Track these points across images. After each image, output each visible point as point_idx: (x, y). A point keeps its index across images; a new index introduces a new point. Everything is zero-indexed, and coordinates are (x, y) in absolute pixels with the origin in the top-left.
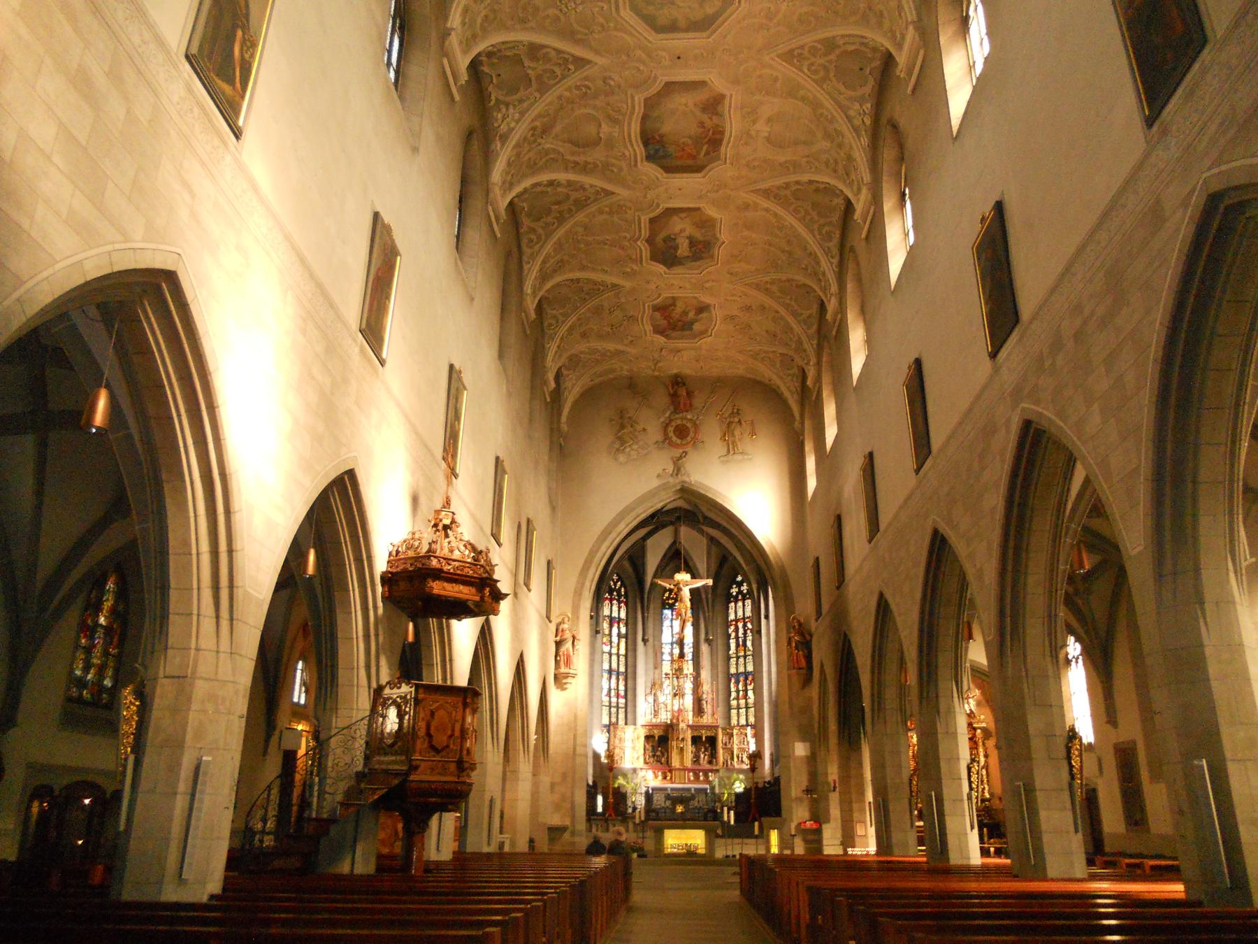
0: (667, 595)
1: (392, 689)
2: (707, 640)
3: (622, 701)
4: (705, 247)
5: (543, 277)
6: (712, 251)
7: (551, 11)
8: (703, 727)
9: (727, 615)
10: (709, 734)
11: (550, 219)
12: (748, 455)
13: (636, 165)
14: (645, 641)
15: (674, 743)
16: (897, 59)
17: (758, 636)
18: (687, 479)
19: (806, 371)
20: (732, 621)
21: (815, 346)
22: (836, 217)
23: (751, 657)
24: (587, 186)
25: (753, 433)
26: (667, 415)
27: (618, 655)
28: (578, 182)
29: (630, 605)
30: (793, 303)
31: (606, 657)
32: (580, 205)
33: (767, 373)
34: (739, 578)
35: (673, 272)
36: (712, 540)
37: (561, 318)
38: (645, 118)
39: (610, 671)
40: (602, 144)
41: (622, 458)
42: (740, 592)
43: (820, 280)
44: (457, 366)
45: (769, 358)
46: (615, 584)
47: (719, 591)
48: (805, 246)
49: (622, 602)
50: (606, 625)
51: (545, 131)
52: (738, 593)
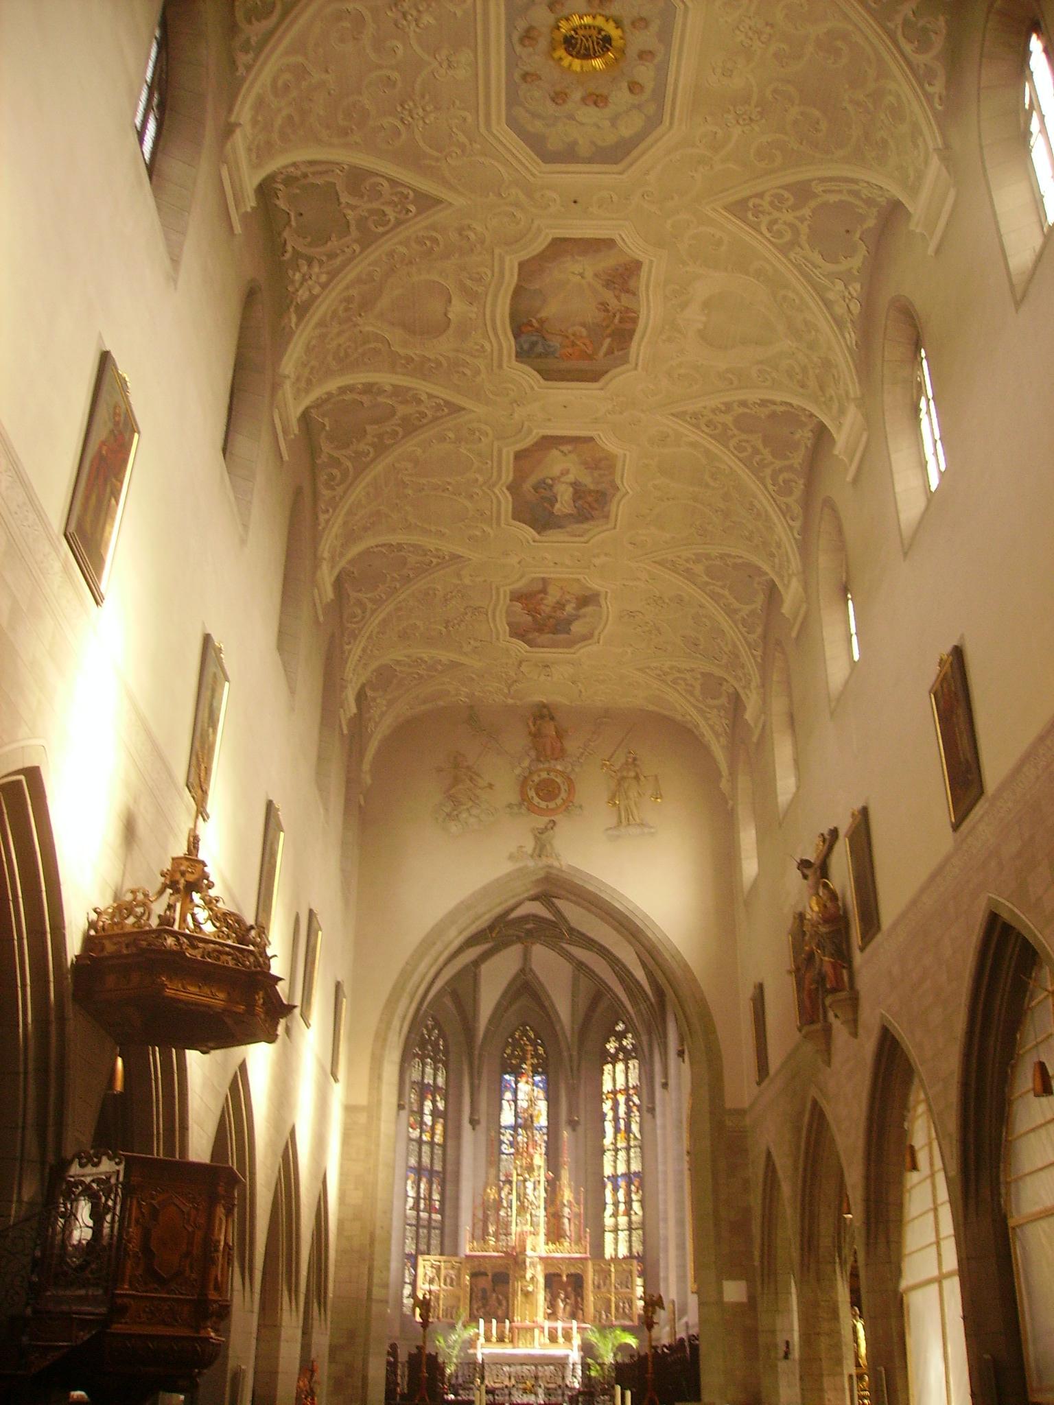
0: (508, 1051)
1: (82, 1166)
4: (596, 501)
5: (350, 537)
6: (606, 509)
7: (388, 121)
10: (573, 1271)
11: (362, 447)
12: (652, 827)
13: (500, 366)
14: (474, 1122)
15: (519, 1285)
16: (911, 210)
18: (556, 864)
19: (743, 697)
21: (759, 660)
22: (798, 459)
23: (638, 1150)
24: (424, 397)
25: (658, 795)
26: (526, 763)
27: (432, 1144)
28: (410, 389)
30: (726, 593)
31: (414, 1146)
32: (410, 427)
33: (682, 706)
34: (620, 1027)
35: (544, 539)
36: (580, 966)
37: (370, 605)
38: (518, 292)
40: (451, 331)
41: (454, 828)
42: (621, 1048)
43: (773, 555)
44: (217, 640)
45: (685, 680)
48: (751, 503)
49: (440, 1061)
51: (366, 305)
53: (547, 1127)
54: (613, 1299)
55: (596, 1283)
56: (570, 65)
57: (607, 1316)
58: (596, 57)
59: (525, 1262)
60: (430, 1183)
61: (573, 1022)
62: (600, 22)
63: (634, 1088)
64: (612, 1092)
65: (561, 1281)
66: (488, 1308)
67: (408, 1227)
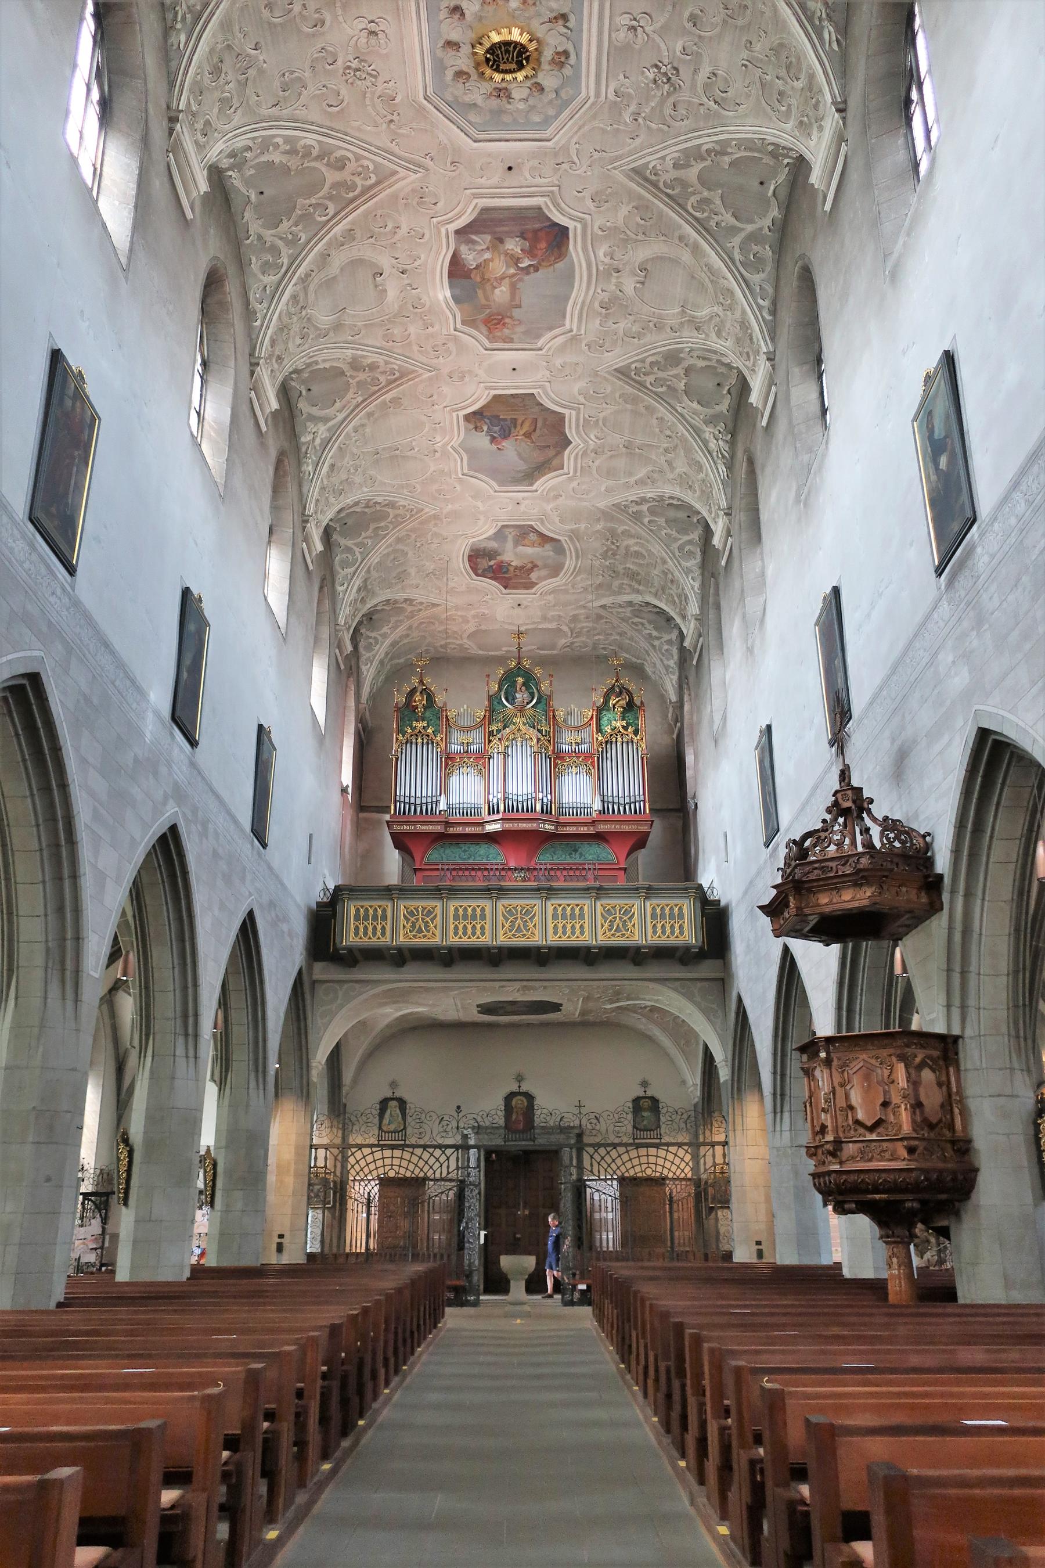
56: (521, 34)
58: (499, 43)
62: (498, 77)
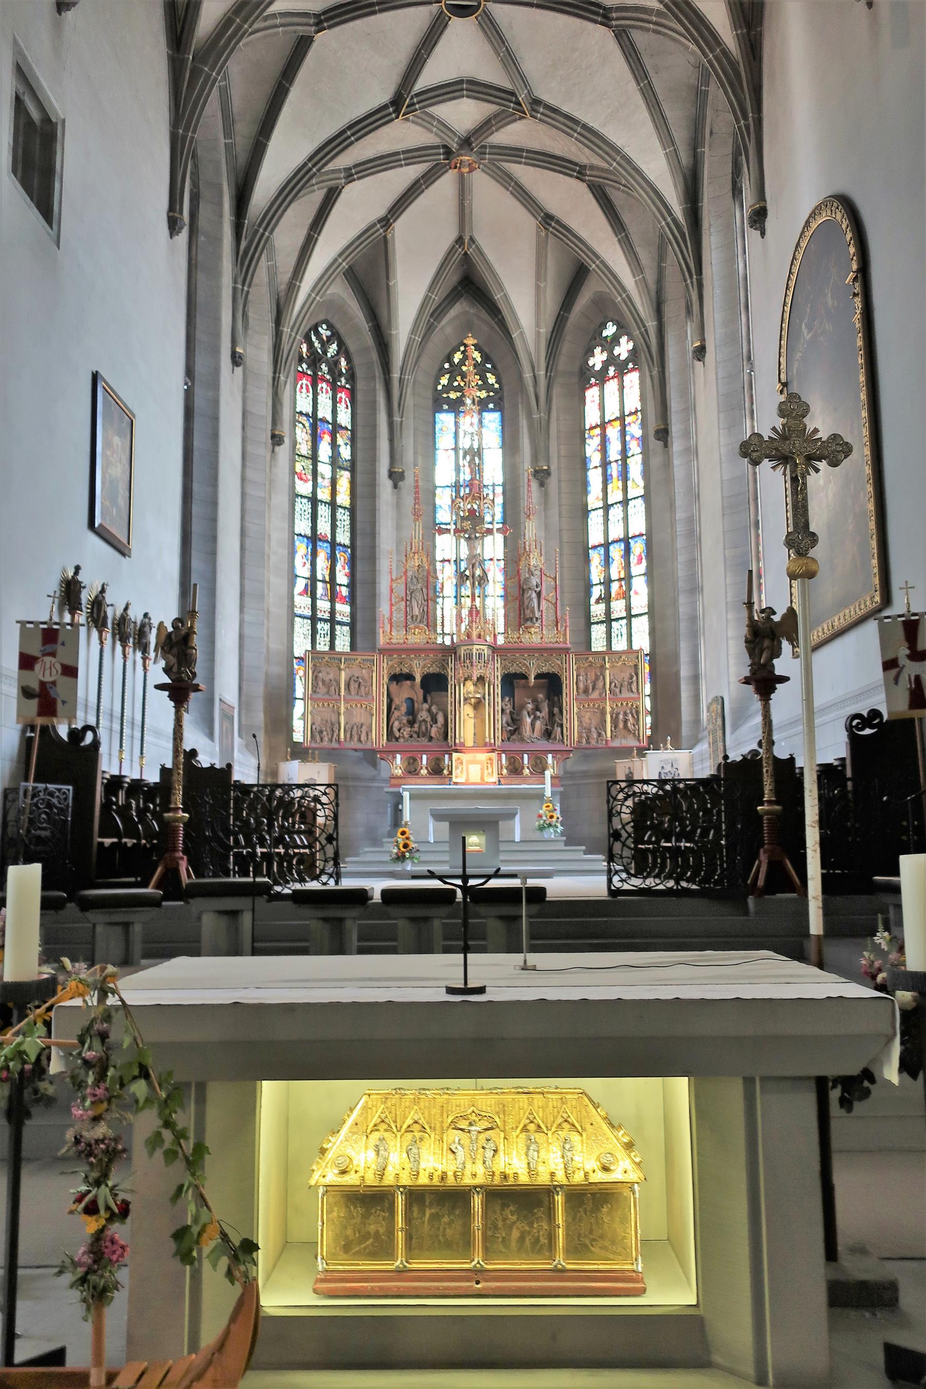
0: (444, 381)
2: (541, 476)
3: (343, 609)
8: (532, 651)
9: (581, 415)
14: (396, 477)
17: (660, 444)
20: (592, 428)
27: (333, 505)
29: (359, 397)
31: (303, 507)
34: (610, 330)
36: (547, 219)
39: (314, 539)
46: (325, 344)
47: (562, 363)
50: (302, 436)
52: (606, 365)
53: (504, 485)
54: (608, 709)
55: (581, 685)
57: (599, 735)
59: (470, 656)
60: (333, 559)
61: (538, 325)
63: (631, 414)
64: (597, 426)
65: (526, 687)
66: (416, 725)
67: (297, 619)
